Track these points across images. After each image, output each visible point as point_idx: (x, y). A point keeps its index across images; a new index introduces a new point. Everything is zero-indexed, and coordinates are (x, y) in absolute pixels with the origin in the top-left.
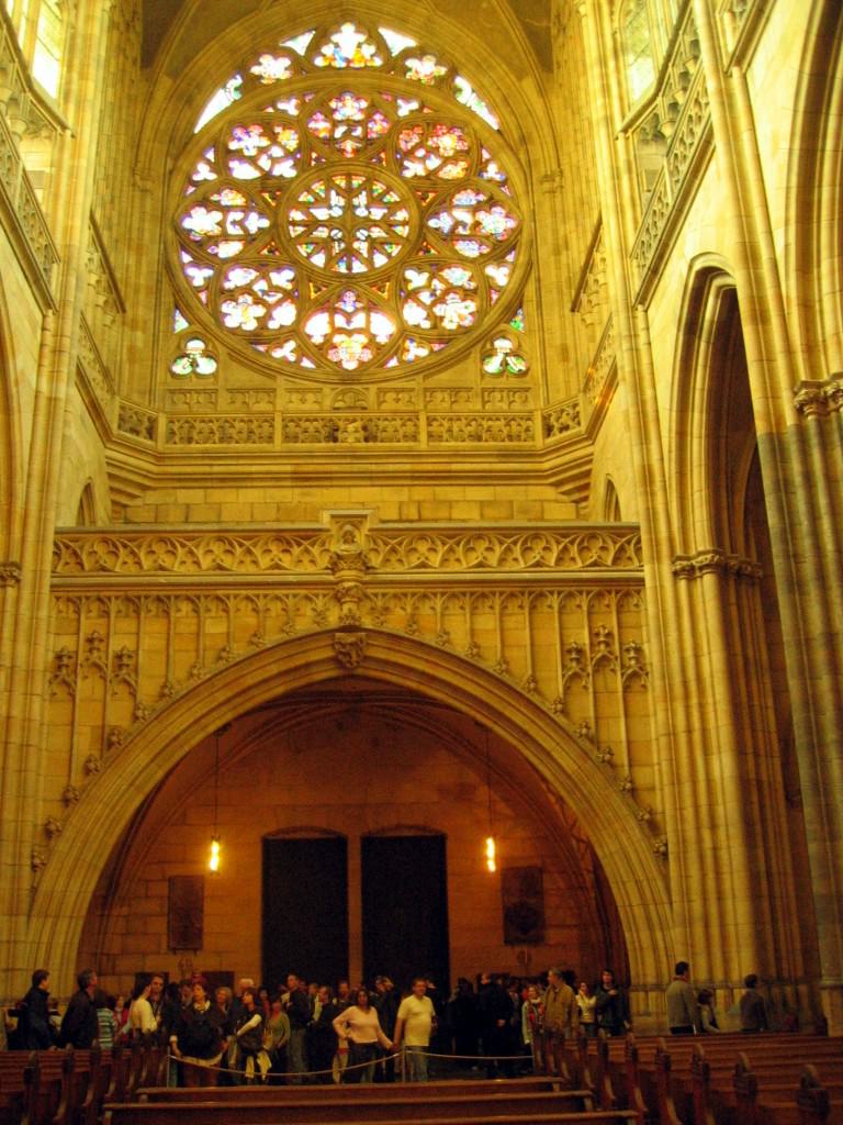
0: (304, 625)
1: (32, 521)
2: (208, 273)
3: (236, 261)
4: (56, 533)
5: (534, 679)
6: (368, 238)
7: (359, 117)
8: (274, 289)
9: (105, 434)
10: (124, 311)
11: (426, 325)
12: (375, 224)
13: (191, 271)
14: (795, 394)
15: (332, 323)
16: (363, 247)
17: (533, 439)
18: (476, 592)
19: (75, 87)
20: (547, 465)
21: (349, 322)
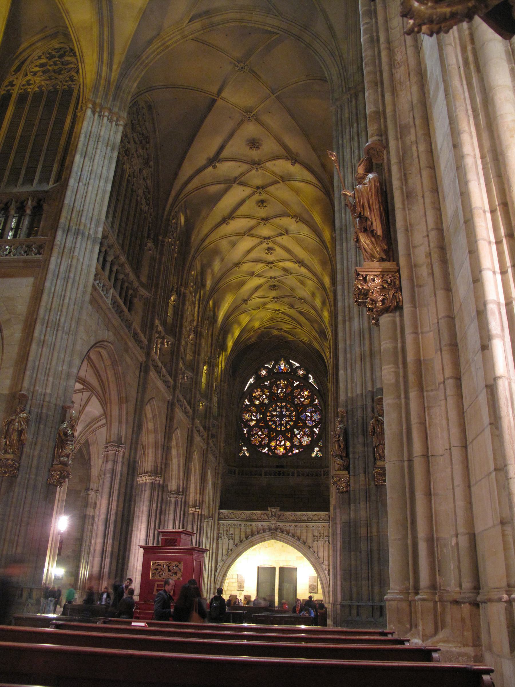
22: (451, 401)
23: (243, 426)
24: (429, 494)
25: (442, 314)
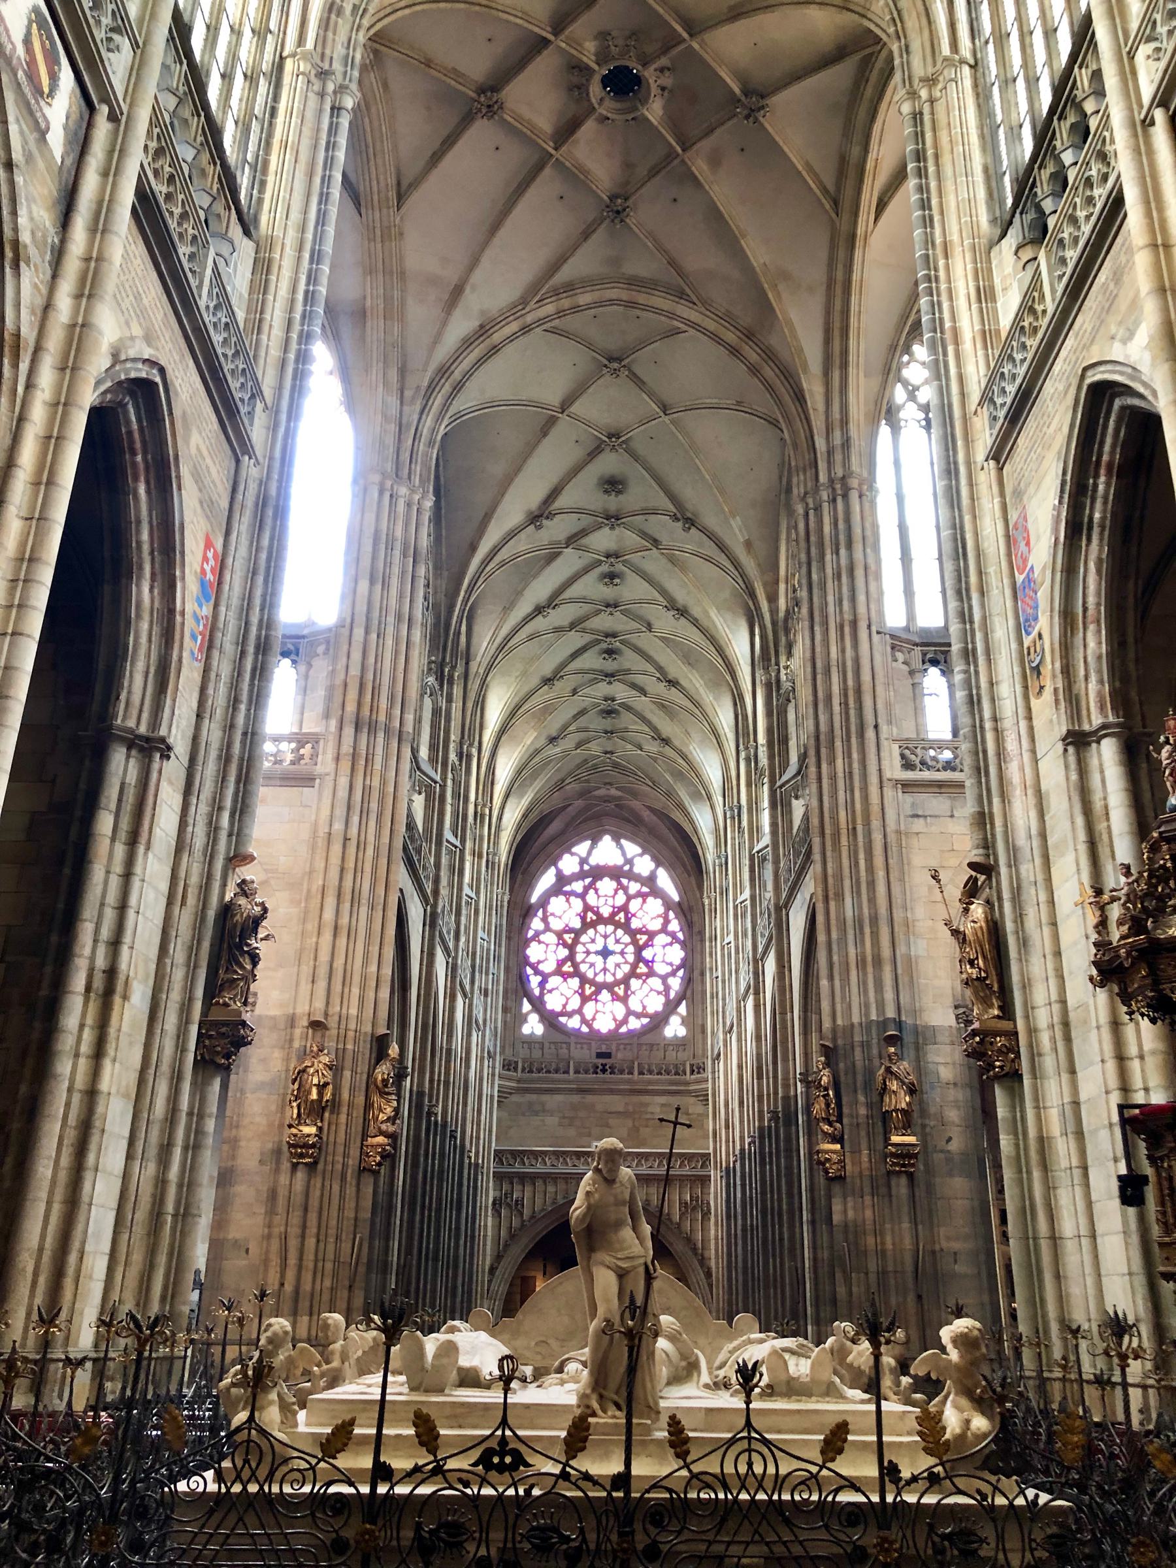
22: (1078, 1191)
24: (1058, 1277)
25: (1067, 1100)
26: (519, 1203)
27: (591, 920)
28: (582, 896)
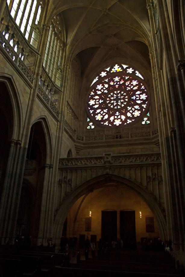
0: (100, 174)
1: (55, 157)
2: (93, 111)
3: (98, 108)
4: (59, 159)
5: (141, 182)
6: (120, 102)
7: (119, 80)
8: (104, 112)
9: (73, 140)
10: (78, 119)
11: (131, 116)
12: (122, 99)
13: (91, 111)
14: (170, 130)
15: (114, 117)
16: (119, 103)
17: (151, 136)
18: (130, 167)
19: (63, 85)
20: (153, 141)
21: (117, 117)
23: (89, 108)
26: (70, 180)
27: (111, 89)
28: (108, 83)
